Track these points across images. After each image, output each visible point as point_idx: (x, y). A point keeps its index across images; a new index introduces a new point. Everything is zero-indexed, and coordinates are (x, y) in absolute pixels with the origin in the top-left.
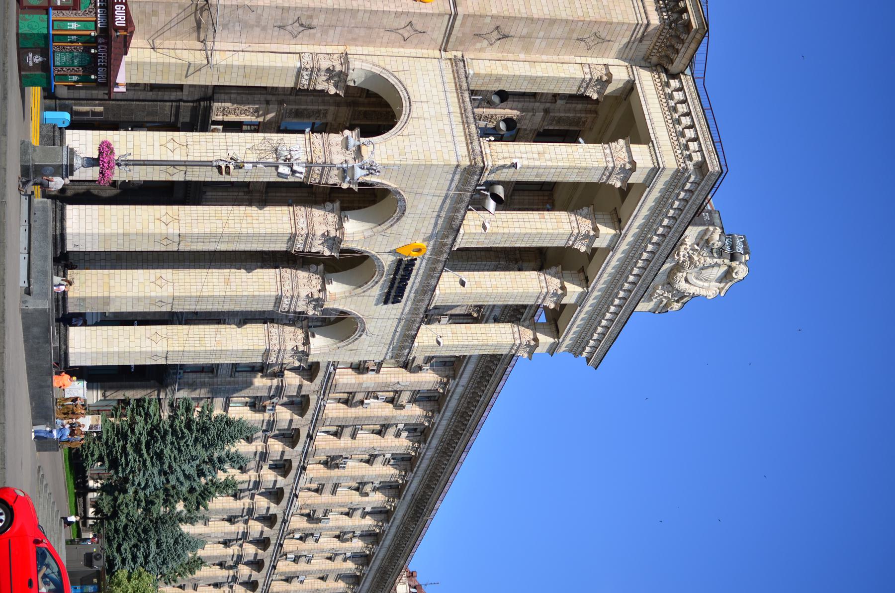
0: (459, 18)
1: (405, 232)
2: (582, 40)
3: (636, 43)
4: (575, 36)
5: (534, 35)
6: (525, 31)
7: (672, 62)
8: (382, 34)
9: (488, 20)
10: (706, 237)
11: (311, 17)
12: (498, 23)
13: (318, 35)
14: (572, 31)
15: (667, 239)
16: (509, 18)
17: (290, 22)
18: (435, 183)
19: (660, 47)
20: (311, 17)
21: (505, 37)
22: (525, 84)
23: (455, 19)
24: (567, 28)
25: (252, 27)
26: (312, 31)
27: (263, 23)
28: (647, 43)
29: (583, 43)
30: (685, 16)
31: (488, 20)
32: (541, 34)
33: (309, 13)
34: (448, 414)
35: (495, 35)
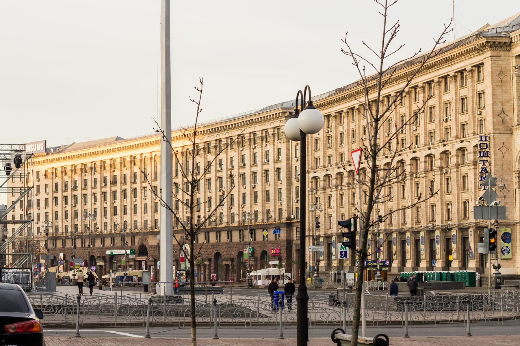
0: (494, 132)
2: (501, 81)
4: (500, 84)
6: (500, 104)
7: (505, 43)
9: (495, 120)
12: (496, 116)
13: (508, 183)
14: (498, 86)
16: (493, 112)
17: (502, 194)
21: (503, 110)
24: (496, 88)
26: (506, 185)
28: (501, 53)
31: (495, 120)
32: (500, 98)
35: (503, 115)
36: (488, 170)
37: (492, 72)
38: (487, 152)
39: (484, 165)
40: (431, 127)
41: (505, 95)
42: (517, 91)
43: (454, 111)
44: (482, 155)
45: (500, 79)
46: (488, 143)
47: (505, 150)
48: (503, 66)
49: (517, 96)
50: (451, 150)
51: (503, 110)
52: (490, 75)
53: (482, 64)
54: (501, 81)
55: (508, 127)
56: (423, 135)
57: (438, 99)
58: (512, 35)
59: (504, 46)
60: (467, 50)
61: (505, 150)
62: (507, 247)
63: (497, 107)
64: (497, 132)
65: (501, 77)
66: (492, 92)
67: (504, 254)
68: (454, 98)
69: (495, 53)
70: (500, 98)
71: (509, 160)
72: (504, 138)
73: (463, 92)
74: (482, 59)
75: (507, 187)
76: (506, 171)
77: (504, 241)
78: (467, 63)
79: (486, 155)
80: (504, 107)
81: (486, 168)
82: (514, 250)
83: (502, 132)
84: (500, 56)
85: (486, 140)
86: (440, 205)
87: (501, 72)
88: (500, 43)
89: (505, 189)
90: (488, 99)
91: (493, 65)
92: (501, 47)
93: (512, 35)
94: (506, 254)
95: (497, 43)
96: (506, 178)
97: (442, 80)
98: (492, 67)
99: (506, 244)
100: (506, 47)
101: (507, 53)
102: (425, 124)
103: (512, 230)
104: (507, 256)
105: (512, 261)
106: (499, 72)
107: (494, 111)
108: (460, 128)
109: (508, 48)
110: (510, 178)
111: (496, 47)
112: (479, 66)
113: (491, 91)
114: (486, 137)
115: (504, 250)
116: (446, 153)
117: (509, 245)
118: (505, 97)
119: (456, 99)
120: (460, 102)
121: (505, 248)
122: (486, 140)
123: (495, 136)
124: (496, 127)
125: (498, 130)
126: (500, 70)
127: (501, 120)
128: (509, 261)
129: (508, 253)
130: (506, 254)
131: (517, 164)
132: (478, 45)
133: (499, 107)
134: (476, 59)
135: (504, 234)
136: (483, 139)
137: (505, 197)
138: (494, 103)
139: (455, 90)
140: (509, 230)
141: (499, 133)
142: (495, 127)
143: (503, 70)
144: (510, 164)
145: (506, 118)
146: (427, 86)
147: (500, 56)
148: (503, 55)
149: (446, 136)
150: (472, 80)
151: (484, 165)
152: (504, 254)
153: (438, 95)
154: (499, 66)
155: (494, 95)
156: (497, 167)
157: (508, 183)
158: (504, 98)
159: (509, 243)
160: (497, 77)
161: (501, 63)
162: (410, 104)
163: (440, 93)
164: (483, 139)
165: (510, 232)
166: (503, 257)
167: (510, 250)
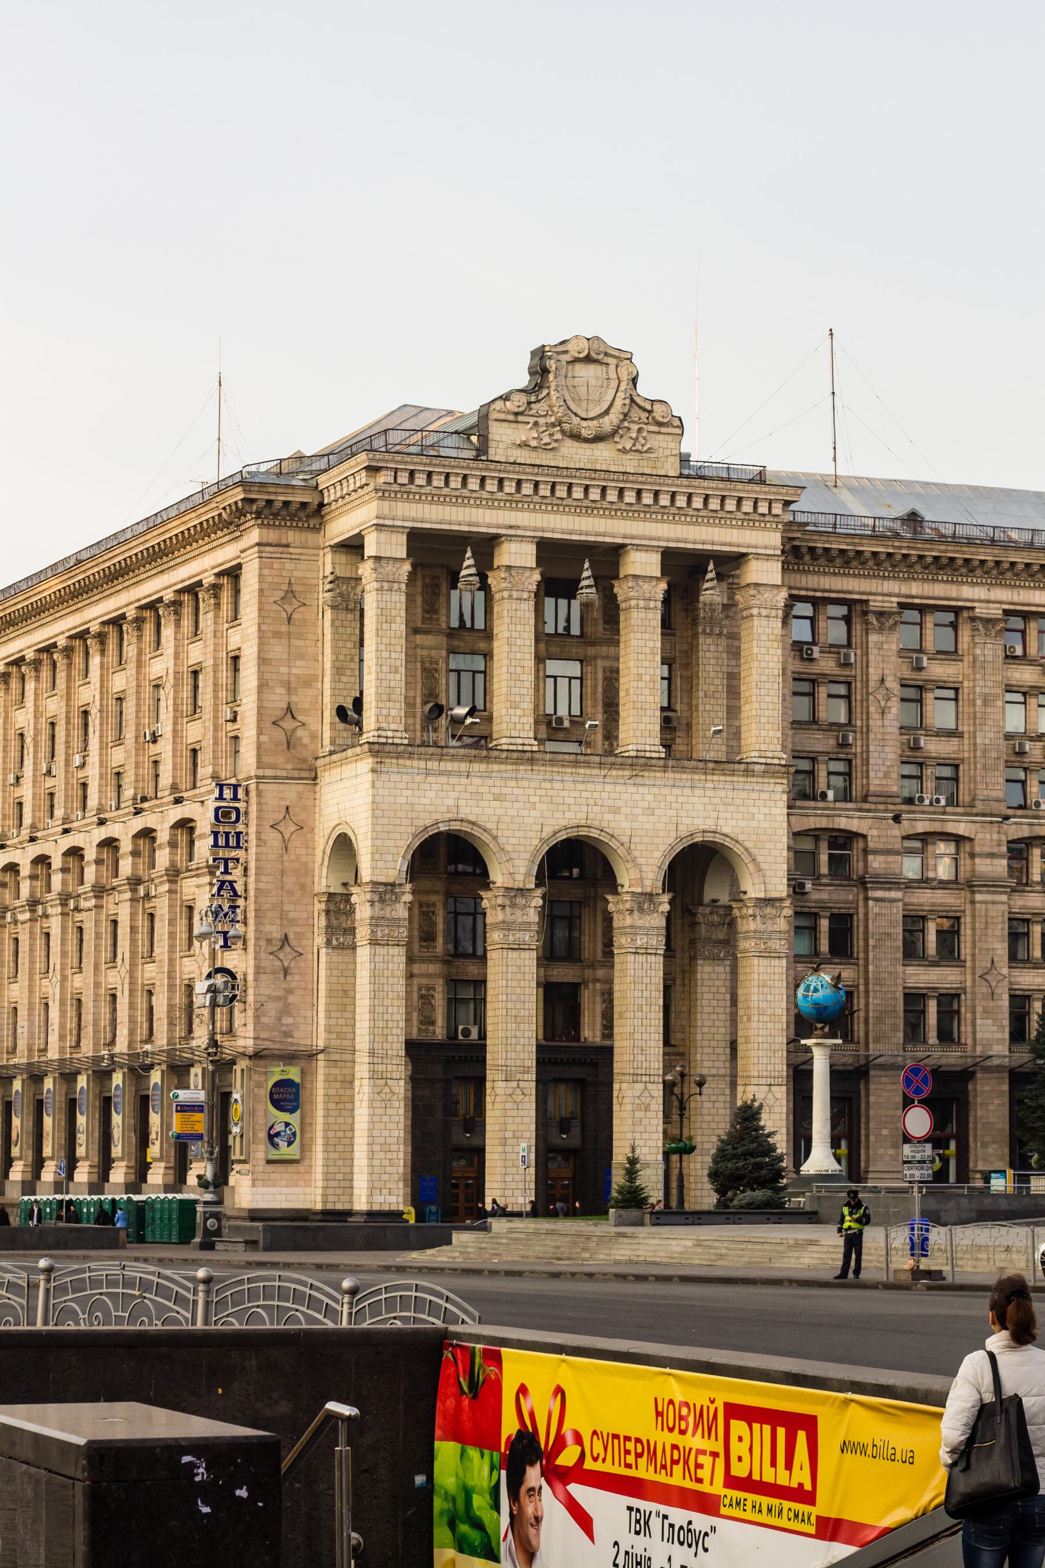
0: (260, 773)
1: (500, 812)
2: (289, 619)
3: (291, 550)
4: (284, 628)
5: (285, 678)
6: (281, 691)
7: (304, 505)
8: (293, 857)
10: (511, 417)
11: (269, 941)
12: (269, 725)
14: (277, 635)
15: (502, 475)
17: (278, 963)
18: (405, 793)
19: (292, 520)
20: (269, 941)
21: (289, 709)
22: (344, 679)
23: (263, 777)
24: (272, 641)
25: (287, 1005)
26: (291, 936)
27: (281, 993)
28: (291, 536)
29: (295, 616)
32: (284, 670)
33: (263, 943)
35: (288, 724)
36: (239, 888)
37: (261, 591)
38: (238, 834)
39: (226, 872)
40: (118, 756)
41: (299, 663)
42: (333, 653)
43: (171, 708)
44: (221, 841)
45: (284, 615)
46: (240, 805)
47: (293, 828)
48: (296, 574)
49: (333, 666)
50: (158, 828)
51: (289, 709)
52: (255, 601)
53: (239, 566)
54: (289, 619)
55: (304, 760)
56: (96, 783)
57: (134, 671)
58: (323, 481)
59: (302, 514)
60: (201, 523)
61: (293, 828)
62: (287, 1124)
63: (271, 697)
64: (268, 772)
65: (290, 610)
66: (259, 652)
67: (275, 1146)
68: (171, 671)
69: (272, 536)
70: (284, 670)
71: (304, 859)
72: (291, 792)
73: (196, 653)
75: (293, 943)
76: (291, 893)
77: (278, 1104)
78: (202, 565)
79: (232, 842)
80: (294, 699)
81: (231, 883)
82: (307, 1135)
83: (284, 774)
84: (287, 546)
85: (235, 798)
86: (127, 993)
87: (290, 593)
88: (286, 504)
89: (287, 949)
91: (266, 572)
92: (292, 517)
93: (323, 481)
94: (283, 1144)
95: (278, 505)
96: (292, 915)
97: (147, 614)
98: (261, 575)
99: (285, 1117)
100: (308, 516)
101: (311, 538)
102: (103, 747)
103: (303, 1072)
104: (285, 1151)
105: (301, 1168)
106: (282, 594)
107: (261, 710)
108: (186, 761)
109: (313, 522)
110: (304, 915)
111: (276, 515)
112: (233, 573)
113: (255, 649)
114: (235, 787)
115: (278, 1134)
116: (147, 834)
117: (294, 1119)
118: (299, 668)
119: (176, 673)
120: (188, 681)
121: (279, 1128)
122: (235, 798)
123: (261, 786)
124: (267, 759)
125: (273, 767)
126: (285, 587)
127: (280, 736)
128: (291, 1168)
129: (290, 1143)
130: (283, 1144)
131: (324, 874)
132: (224, 508)
133: (278, 699)
134: (224, 555)
135: (278, 1084)
136: (228, 793)
137: (286, 972)
138: (263, 686)
139: (176, 646)
140: (293, 1073)
141: (276, 777)
142: (264, 759)
143: (295, 588)
144: (306, 871)
145: (300, 733)
146: (112, 632)
147: (287, 546)
148: (298, 544)
149: (152, 784)
150: (216, 617)
151: (226, 872)
152: (275, 1146)
153: (134, 659)
154: (284, 573)
155: (263, 661)
156: (263, 878)
157: (297, 929)
158: (294, 671)
159: (292, 1111)
160: (276, 607)
161: (289, 565)
162: (68, 688)
163: (140, 654)
164: (228, 793)
165: (297, 1080)
166: (274, 1154)
167: (294, 1134)
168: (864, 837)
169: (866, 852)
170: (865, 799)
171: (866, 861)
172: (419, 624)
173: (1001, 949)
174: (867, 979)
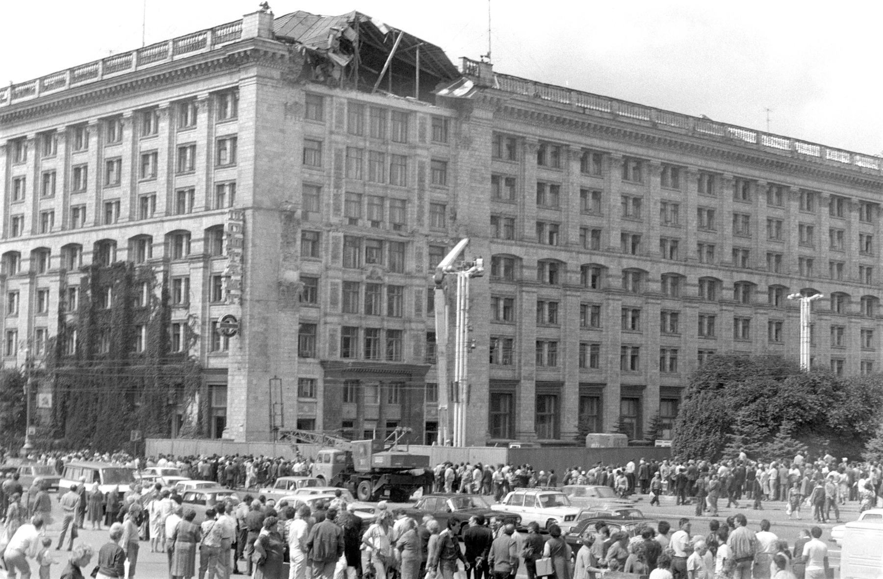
14: (264, 128)
30: (249, 53)
34: (651, 153)
37: (257, 102)
50: (154, 235)
52: (252, 109)
56: (93, 207)
66: (256, 136)
69: (263, 72)
74: (236, 80)
90: (246, 149)
97: (139, 114)
98: (257, 93)
102: (98, 187)
113: (253, 135)
134: (223, 82)
139: (170, 133)
153: (130, 139)
168: (521, 259)
169: (522, 267)
170: (521, 240)
171: (522, 272)
172: (334, 129)
173: (577, 320)
174: (521, 334)
